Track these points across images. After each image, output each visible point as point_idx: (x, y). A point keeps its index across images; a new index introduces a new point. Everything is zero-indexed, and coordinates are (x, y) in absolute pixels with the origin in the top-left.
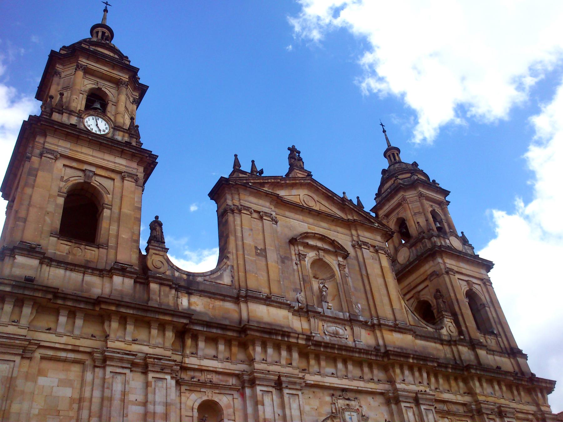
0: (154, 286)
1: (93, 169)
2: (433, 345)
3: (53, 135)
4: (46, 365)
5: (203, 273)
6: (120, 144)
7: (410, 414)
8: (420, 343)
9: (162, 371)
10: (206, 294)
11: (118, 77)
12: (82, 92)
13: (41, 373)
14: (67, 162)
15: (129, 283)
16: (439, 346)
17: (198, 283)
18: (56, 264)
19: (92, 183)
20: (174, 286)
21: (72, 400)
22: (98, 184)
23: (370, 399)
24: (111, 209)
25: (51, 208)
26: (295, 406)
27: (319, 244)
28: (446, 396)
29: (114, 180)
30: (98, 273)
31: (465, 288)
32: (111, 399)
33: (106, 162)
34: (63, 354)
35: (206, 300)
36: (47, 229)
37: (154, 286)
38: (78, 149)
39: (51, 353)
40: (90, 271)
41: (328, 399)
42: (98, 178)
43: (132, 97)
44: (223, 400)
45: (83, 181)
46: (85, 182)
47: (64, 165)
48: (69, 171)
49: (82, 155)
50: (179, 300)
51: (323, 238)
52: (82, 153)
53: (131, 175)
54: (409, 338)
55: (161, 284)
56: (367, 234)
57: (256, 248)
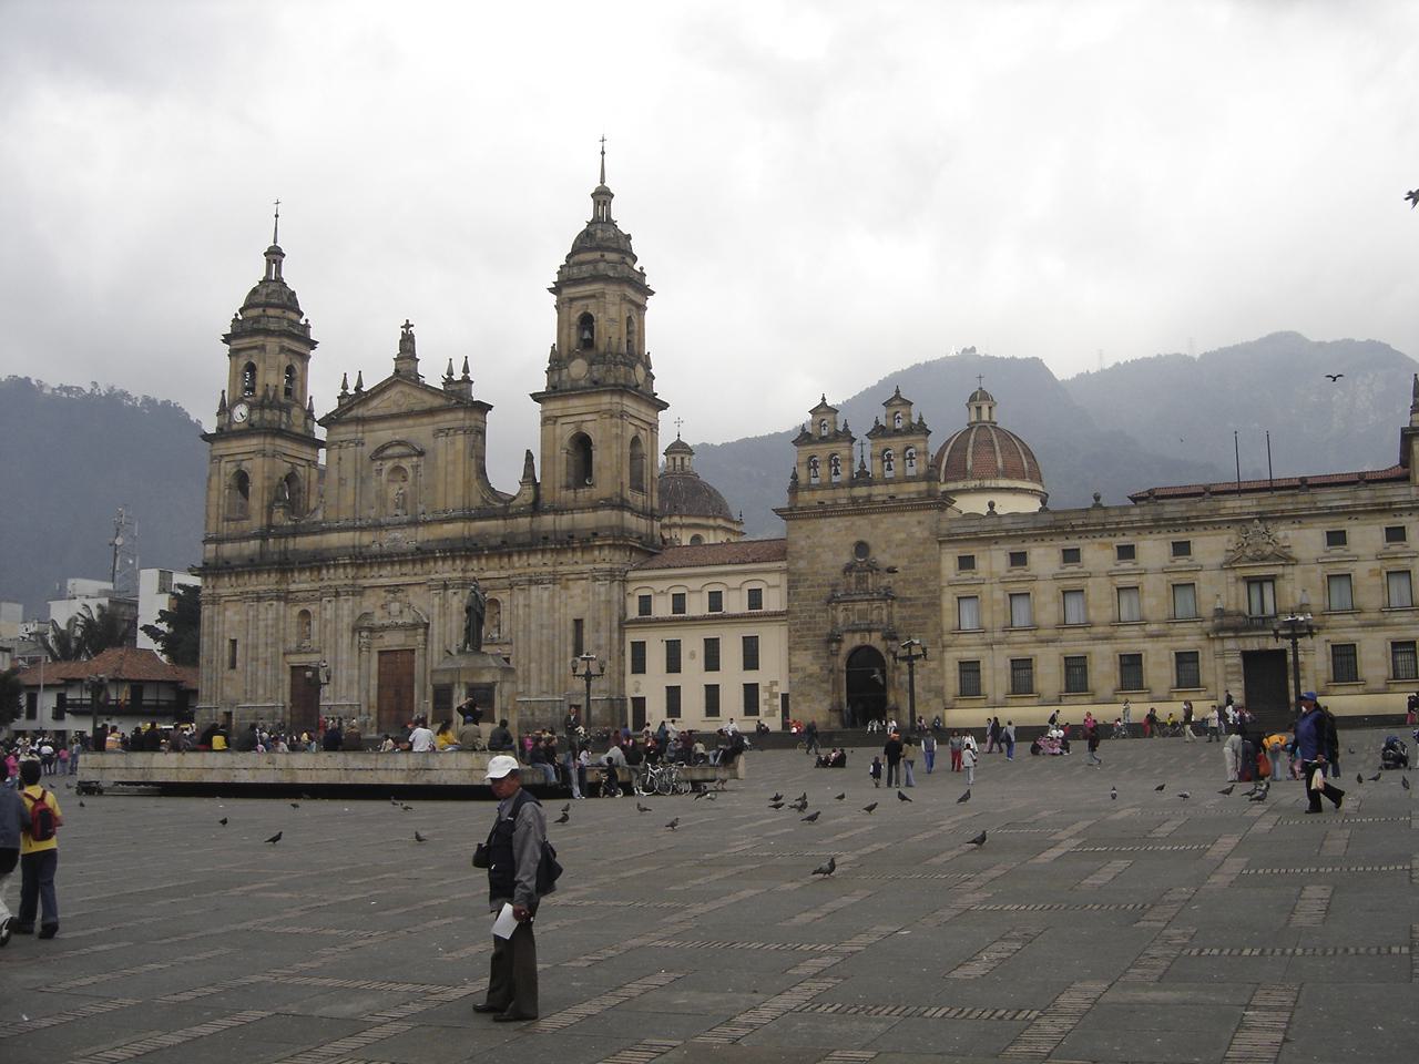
1: (240, 457)
2: (493, 523)
4: (228, 604)
7: (437, 599)
9: (271, 599)
13: (225, 609)
14: (227, 459)
15: (258, 542)
16: (501, 522)
23: (417, 588)
25: (221, 502)
26: (346, 607)
27: (398, 450)
28: (488, 574)
31: (569, 431)
32: (248, 621)
39: (227, 598)
41: (384, 594)
42: (244, 463)
44: (312, 608)
48: (229, 465)
51: (399, 443)
56: (449, 416)
57: (340, 479)
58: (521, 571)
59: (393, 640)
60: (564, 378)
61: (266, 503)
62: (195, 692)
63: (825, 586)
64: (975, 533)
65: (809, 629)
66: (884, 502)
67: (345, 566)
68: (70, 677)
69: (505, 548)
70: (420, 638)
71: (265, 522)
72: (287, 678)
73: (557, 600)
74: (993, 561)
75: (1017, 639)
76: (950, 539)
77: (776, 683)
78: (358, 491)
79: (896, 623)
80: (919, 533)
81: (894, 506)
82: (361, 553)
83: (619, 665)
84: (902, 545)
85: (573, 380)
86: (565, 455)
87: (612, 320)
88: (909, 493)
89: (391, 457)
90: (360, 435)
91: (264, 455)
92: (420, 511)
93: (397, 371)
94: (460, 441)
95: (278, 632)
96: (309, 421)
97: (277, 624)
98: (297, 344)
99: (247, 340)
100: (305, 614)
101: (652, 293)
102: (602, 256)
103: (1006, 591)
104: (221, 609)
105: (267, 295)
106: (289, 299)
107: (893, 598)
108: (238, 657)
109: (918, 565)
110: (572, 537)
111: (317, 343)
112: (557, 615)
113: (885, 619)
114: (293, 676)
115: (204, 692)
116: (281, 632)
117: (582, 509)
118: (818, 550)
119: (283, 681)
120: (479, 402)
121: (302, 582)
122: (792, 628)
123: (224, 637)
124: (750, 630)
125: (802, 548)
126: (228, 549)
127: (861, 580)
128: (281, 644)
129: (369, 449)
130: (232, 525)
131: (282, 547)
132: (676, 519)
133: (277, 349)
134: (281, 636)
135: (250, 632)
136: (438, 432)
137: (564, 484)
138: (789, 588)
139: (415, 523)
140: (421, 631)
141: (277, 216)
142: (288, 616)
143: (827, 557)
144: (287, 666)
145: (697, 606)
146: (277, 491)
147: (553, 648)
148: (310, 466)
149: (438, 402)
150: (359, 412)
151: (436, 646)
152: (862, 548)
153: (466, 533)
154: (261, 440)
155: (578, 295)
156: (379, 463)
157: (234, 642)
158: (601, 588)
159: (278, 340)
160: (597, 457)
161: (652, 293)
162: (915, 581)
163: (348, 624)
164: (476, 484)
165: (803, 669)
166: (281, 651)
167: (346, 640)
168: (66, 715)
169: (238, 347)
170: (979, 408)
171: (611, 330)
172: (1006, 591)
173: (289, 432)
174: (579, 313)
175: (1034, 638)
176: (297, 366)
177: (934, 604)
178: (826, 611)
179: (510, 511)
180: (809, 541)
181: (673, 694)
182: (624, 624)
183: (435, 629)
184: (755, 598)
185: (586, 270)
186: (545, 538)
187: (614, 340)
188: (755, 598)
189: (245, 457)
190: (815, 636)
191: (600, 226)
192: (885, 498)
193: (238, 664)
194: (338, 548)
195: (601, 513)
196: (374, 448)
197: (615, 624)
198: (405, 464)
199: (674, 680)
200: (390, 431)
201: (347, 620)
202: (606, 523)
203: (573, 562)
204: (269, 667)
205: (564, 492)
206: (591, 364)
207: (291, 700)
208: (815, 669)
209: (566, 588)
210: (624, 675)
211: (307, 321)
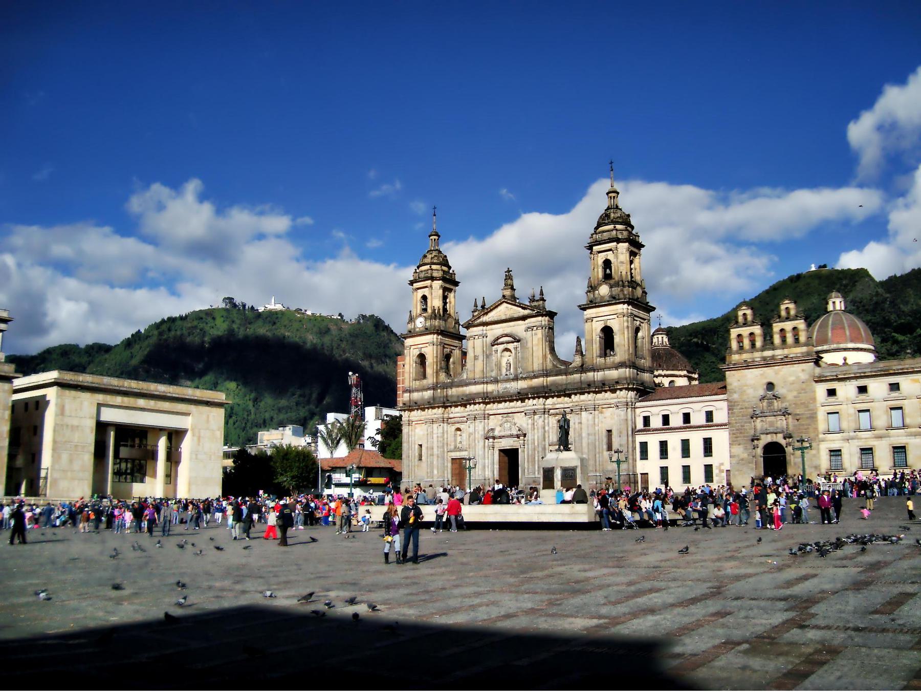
0: (439, 391)
2: (559, 377)
7: (530, 421)
8: (550, 379)
13: (415, 428)
14: (413, 347)
16: (564, 377)
21: (424, 435)
28: (557, 406)
34: (419, 422)
35: (457, 389)
36: (411, 379)
37: (439, 391)
39: (416, 422)
41: (501, 418)
44: (461, 426)
51: (507, 335)
53: (431, 343)
54: (541, 379)
58: (577, 404)
59: (507, 444)
60: (596, 296)
61: (435, 371)
62: (401, 473)
63: (749, 408)
64: (836, 376)
65: (741, 433)
66: (782, 359)
67: (479, 403)
68: (334, 466)
69: (565, 392)
70: (522, 442)
71: (435, 381)
72: (450, 465)
73: (596, 420)
74: (846, 390)
75: (863, 436)
76: (820, 380)
77: (722, 464)
78: (485, 362)
79: (791, 428)
80: (803, 376)
81: (786, 361)
82: (487, 397)
83: (633, 455)
84: (793, 384)
85: (602, 297)
86: (598, 339)
87: (622, 262)
88: (796, 353)
89: (502, 343)
90: (485, 332)
92: (519, 372)
93: (504, 296)
94: (539, 333)
95: (443, 439)
97: (443, 436)
100: (458, 429)
101: (643, 246)
102: (615, 227)
103: (855, 408)
104: (413, 428)
105: (432, 258)
106: (443, 259)
107: (789, 414)
108: (423, 454)
109: (803, 394)
110: (604, 384)
111: (459, 283)
112: (597, 428)
113: (785, 427)
114: (452, 463)
115: (405, 474)
116: (445, 440)
117: (609, 368)
118: (745, 388)
119: (447, 466)
120: (550, 311)
121: (457, 412)
122: (731, 432)
123: (415, 444)
124: (707, 434)
125: (735, 387)
126: (416, 396)
127: (770, 404)
128: (445, 446)
129: (490, 339)
130: (417, 383)
131: (445, 393)
132: (660, 372)
134: (445, 442)
135: (429, 440)
136: (526, 330)
137: (598, 354)
138: (729, 410)
139: (516, 379)
140: (522, 438)
142: (449, 432)
143: (750, 391)
144: (450, 459)
145: (676, 421)
147: (595, 446)
149: (527, 312)
150: (485, 319)
151: (530, 446)
152: (770, 386)
153: (545, 384)
155: (603, 249)
156: (496, 346)
157: (421, 446)
158: (621, 412)
160: (617, 339)
161: (643, 246)
162: (801, 404)
163: (482, 435)
164: (549, 356)
165: (738, 456)
166: (446, 449)
167: (481, 443)
168: (332, 486)
170: (834, 303)
171: (622, 268)
172: (855, 408)
173: (446, 332)
174: (603, 260)
175: (873, 436)
177: (813, 417)
178: (750, 423)
179: (569, 371)
180: (739, 383)
181: (664, 471)
182: (635, 431)
183: (529, 436)
184: (709, 416)
185: (606, 236)
186: (589, 385)
187: (624, 273)
188: (709, 416)
190: (744, 437)
191: (612, 210)
192: (782, 357)
193: (423, 458)
194: (475, 394)
195: (622, 370)
196: (493, 339)
197: (630, 433)
198: (510, 346)
199: (664, 463)
200: (501, 330)
201: (481, 433)
202: (623, 376)
203: (606, 397)
204: (439, 459)
205: (598, 359)
206: (611, 287)
207: (452, 476)
208: (745, 455)
209: (601, 413)
210: (634, 460)
211: (453, 271)
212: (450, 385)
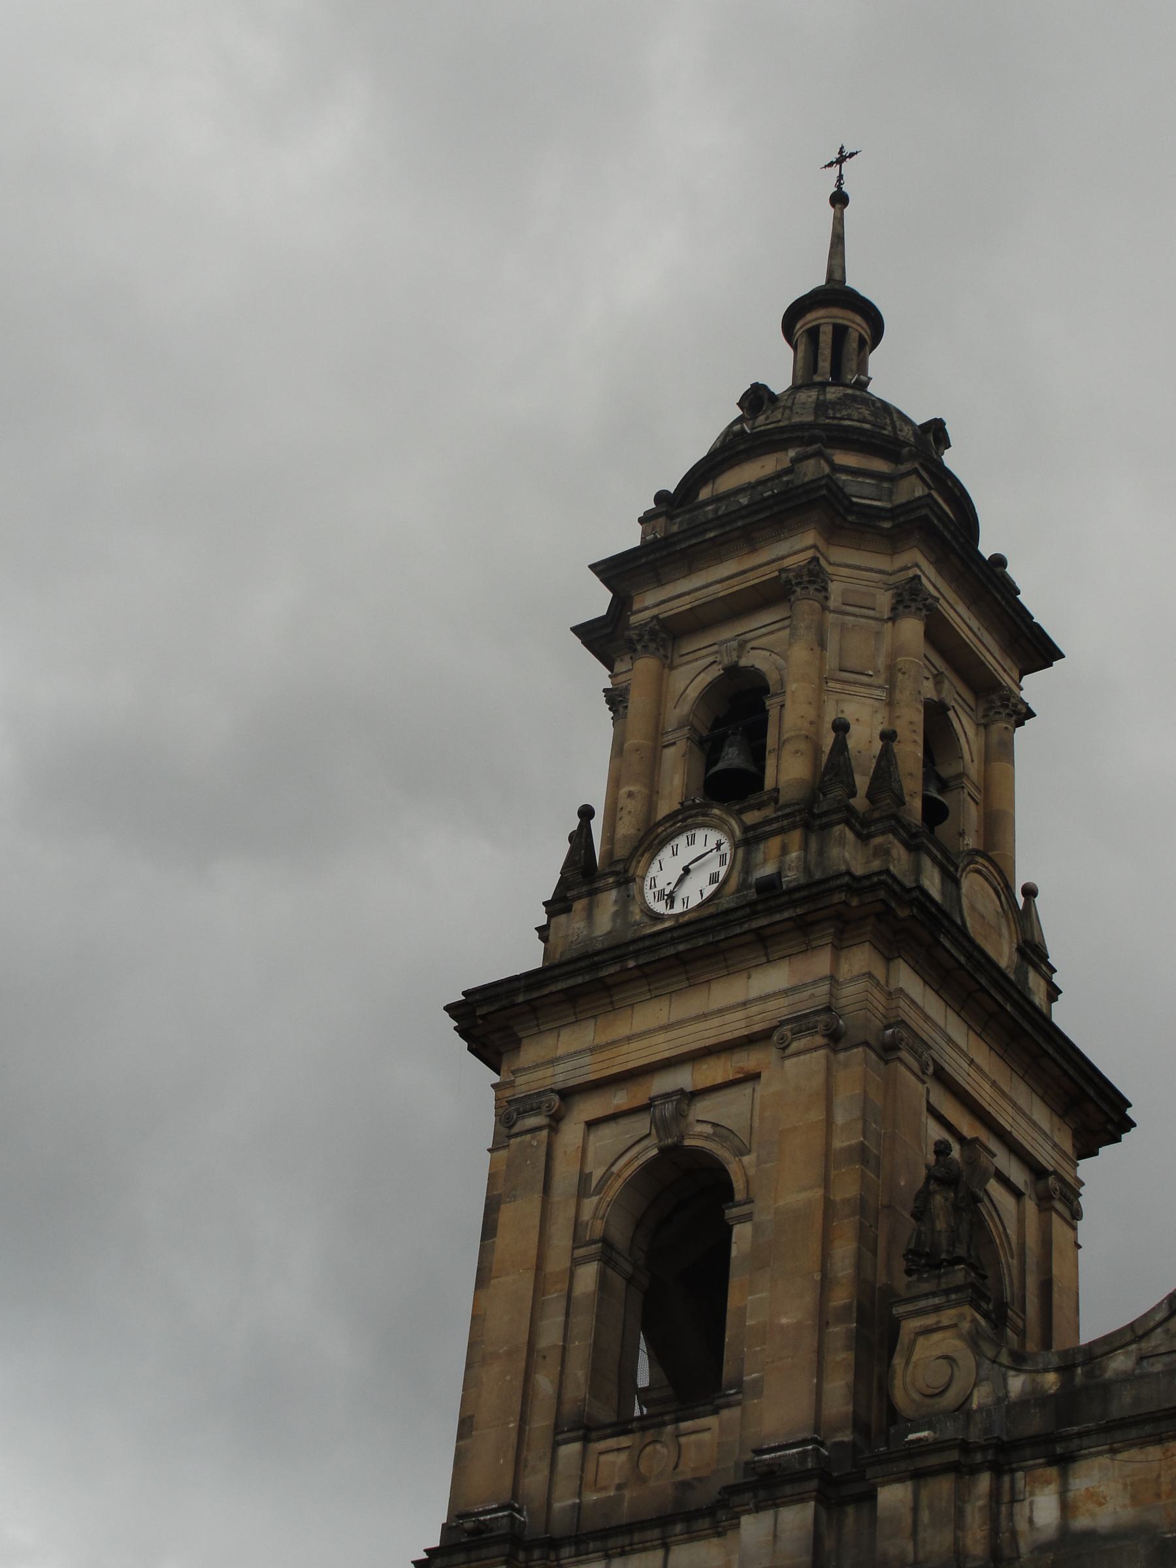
1: (683, 1079)
3: (535, 1030)
5: (1131, 1326)
6: (731, 917)
10: (1134, 1433)
11: (771, 572)
12: (670, 738)
17: (1106, 1389)
18: (572, 1550)
19: (688, 1142)
20: (979, 1458)
22: (708, 1129)
24: (747, 1218)
25: (551, 1334)
29: (754, 1077)
30: (705, 1523)
33: (715, 1022)
36: (541, 1422)
38: (621, 1029)
40: (679, 1528)
42: (703, 1110)
43: (888, 587)
45: (655, 1152)
46: (662, 1150)
47: (591, 1125)
48: (607, 1139)
49: (634, 1046)
50: (1022, 1511)
52: (629, 1039)
53: (801, 1024)
55: (918, 1476)
61: (841, 1296)
91: (835, 1039)
96: (1035, 983)
98: (962, 609)
99: (728, 568)
105: (821, 407)
131: (976, 1538)
133: (884, 601)
141: (839, 199)
146: (921, 1213)
148: (1045, 1202)
154: (820, 963)
159: (881, 562)
169: (683, 605)
176: (964, 725)
189: (715, 1071)
212: (1036, 1423)
